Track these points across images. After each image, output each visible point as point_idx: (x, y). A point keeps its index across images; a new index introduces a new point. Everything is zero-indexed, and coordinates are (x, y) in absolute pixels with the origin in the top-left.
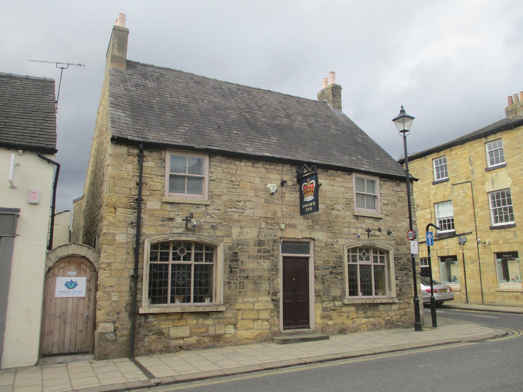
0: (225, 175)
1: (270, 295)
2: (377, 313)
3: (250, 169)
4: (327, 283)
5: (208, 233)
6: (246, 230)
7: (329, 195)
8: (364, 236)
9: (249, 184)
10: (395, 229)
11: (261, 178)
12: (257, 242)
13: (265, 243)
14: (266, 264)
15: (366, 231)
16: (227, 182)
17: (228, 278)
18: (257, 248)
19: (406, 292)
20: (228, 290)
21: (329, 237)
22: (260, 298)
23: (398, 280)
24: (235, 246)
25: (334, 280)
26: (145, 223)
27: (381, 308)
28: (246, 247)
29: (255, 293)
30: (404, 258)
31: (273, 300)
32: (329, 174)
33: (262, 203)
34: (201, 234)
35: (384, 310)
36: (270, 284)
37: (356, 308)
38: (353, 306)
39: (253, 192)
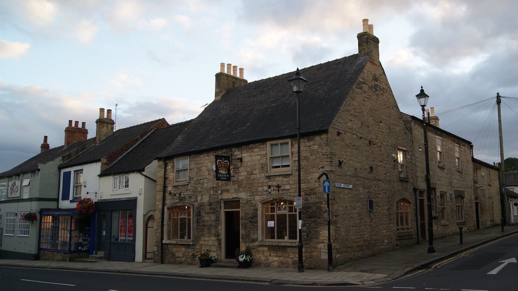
0: (195, 165)
1: (216, 237)
2: (286, 255)
3: (207, 158)
4: (248, 230)
5: (188, 200)
6: (204, 197)
7: (249, 164)
8: (275, 191)
9: (206, 167)
10: (305, 181)
11: (211, 162)
12: (209, 203)
13: (212, 204)
14: (213, 217)
15: (276, 187)
16: (196, 169)
17: (197, 226)
18: (209, 207)
19: (313, 238)
20: (197, 233)
21: (248, 196)
22: (211, 238)
23: (306, 226)
24: (199, 207)
25: (252, 227)
26: (167, 198)
27: (289, 250)
28: (204, 207)
29: (208, 234)
30: (313, 207)
31: (217, 240)
32: (250, 148)
33: (212, 178)
34: (185, 202)
35: (291, 252)
36: (215, 229)
37: (268, 249)
38: (266, 247)
39: (207, 172)
